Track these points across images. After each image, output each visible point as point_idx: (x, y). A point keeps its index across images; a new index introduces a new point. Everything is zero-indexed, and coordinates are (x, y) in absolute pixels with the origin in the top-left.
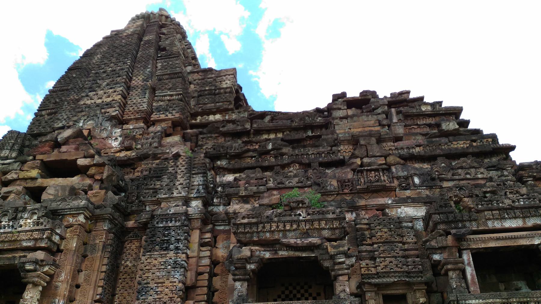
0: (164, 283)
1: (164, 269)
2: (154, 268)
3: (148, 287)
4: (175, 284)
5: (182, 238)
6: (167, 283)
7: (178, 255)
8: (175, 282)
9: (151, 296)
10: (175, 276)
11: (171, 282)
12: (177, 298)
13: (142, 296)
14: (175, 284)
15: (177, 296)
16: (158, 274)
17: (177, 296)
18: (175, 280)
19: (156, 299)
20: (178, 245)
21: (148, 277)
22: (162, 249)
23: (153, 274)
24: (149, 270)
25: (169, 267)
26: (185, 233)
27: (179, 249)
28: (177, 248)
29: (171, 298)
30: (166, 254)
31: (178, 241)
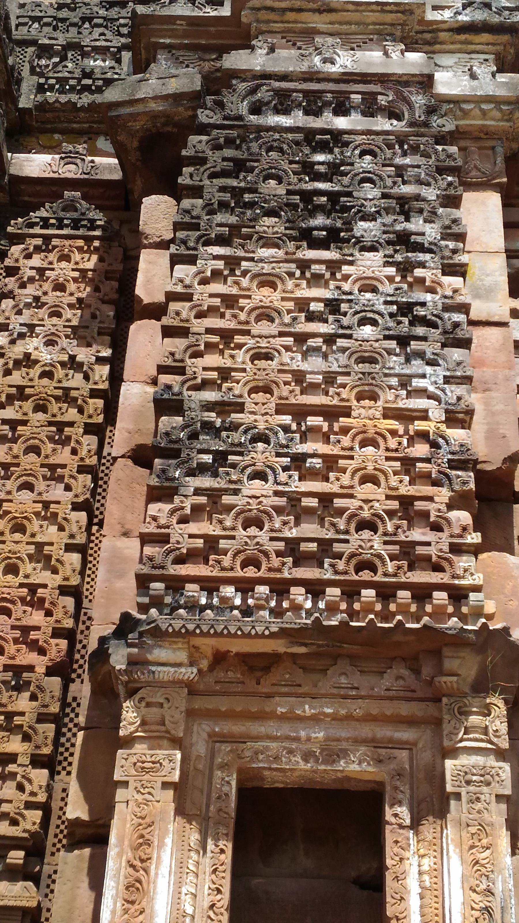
0: (347, 413)
1: (330, 339)
2: (263, 328)
3: (234, 427)
4: (420, 425)
5: (431, 193)
6: (365, 415)
7: (419, 272)
8: (424, 415)
9: (260, 476)
10: (417, 383)
11: (388, 413)
12: (450, 507)
13: (191, 473)
14: (420, 425)
15: (443, 494)
16: (297, 362)
17: (443, 494)
18: (421, 403)
19: (294, 499)
20: (411, 226)
21: (225, 374)
22: (307, 237)
23: (256, 357)
24: (227, 335)
25: (367, 330)
26: (441, 171)
27: (420, 248)
28: (404, 240)
29: (407, 502)
30: (334, 266)
31: (405, 207)
